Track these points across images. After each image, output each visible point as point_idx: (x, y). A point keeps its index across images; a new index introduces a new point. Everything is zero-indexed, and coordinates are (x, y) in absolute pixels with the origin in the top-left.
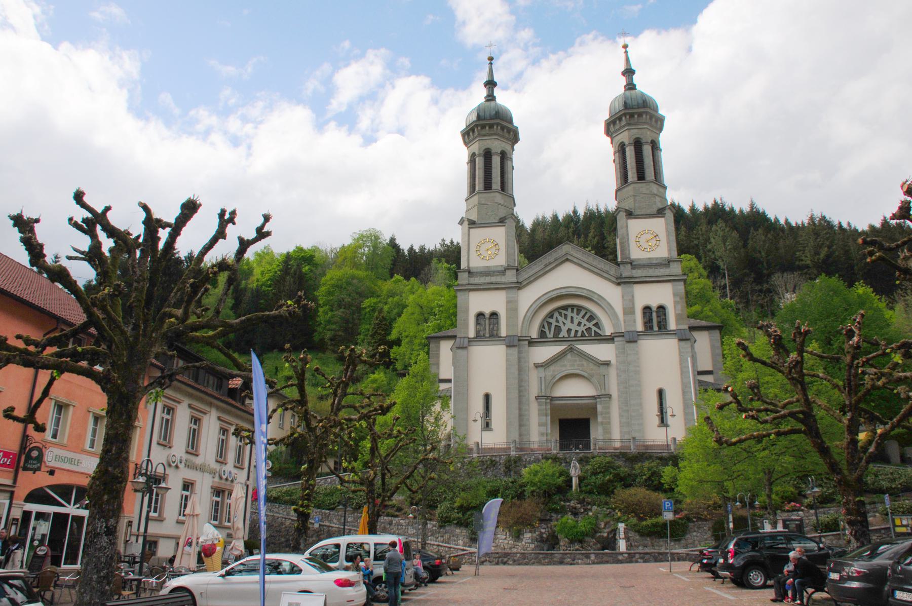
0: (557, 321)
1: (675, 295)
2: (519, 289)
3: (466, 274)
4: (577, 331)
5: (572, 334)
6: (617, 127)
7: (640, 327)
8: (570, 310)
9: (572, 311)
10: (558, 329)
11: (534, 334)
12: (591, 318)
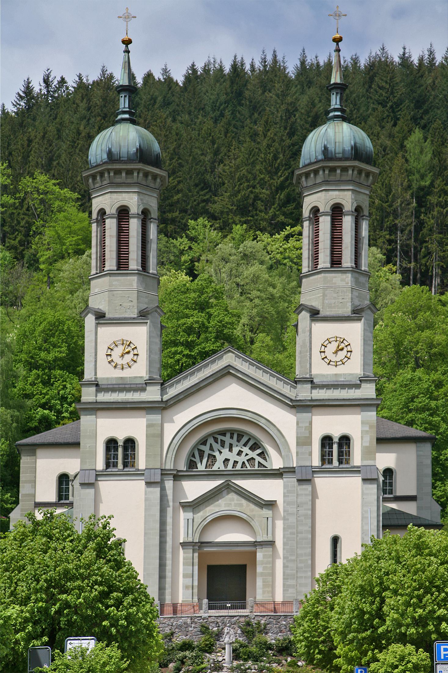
0: (211, 448)
4: (236, 462)
5: (230, 467)
8: (228, 435)
9: (232, 437)
10: (212, 458)
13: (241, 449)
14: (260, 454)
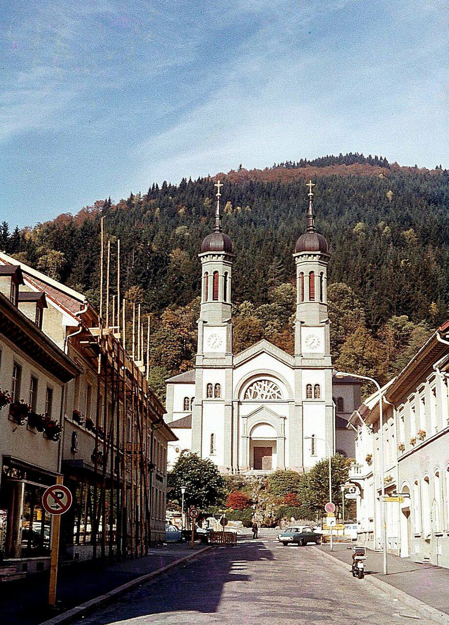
0: (255, 389)
10: (256, 394)
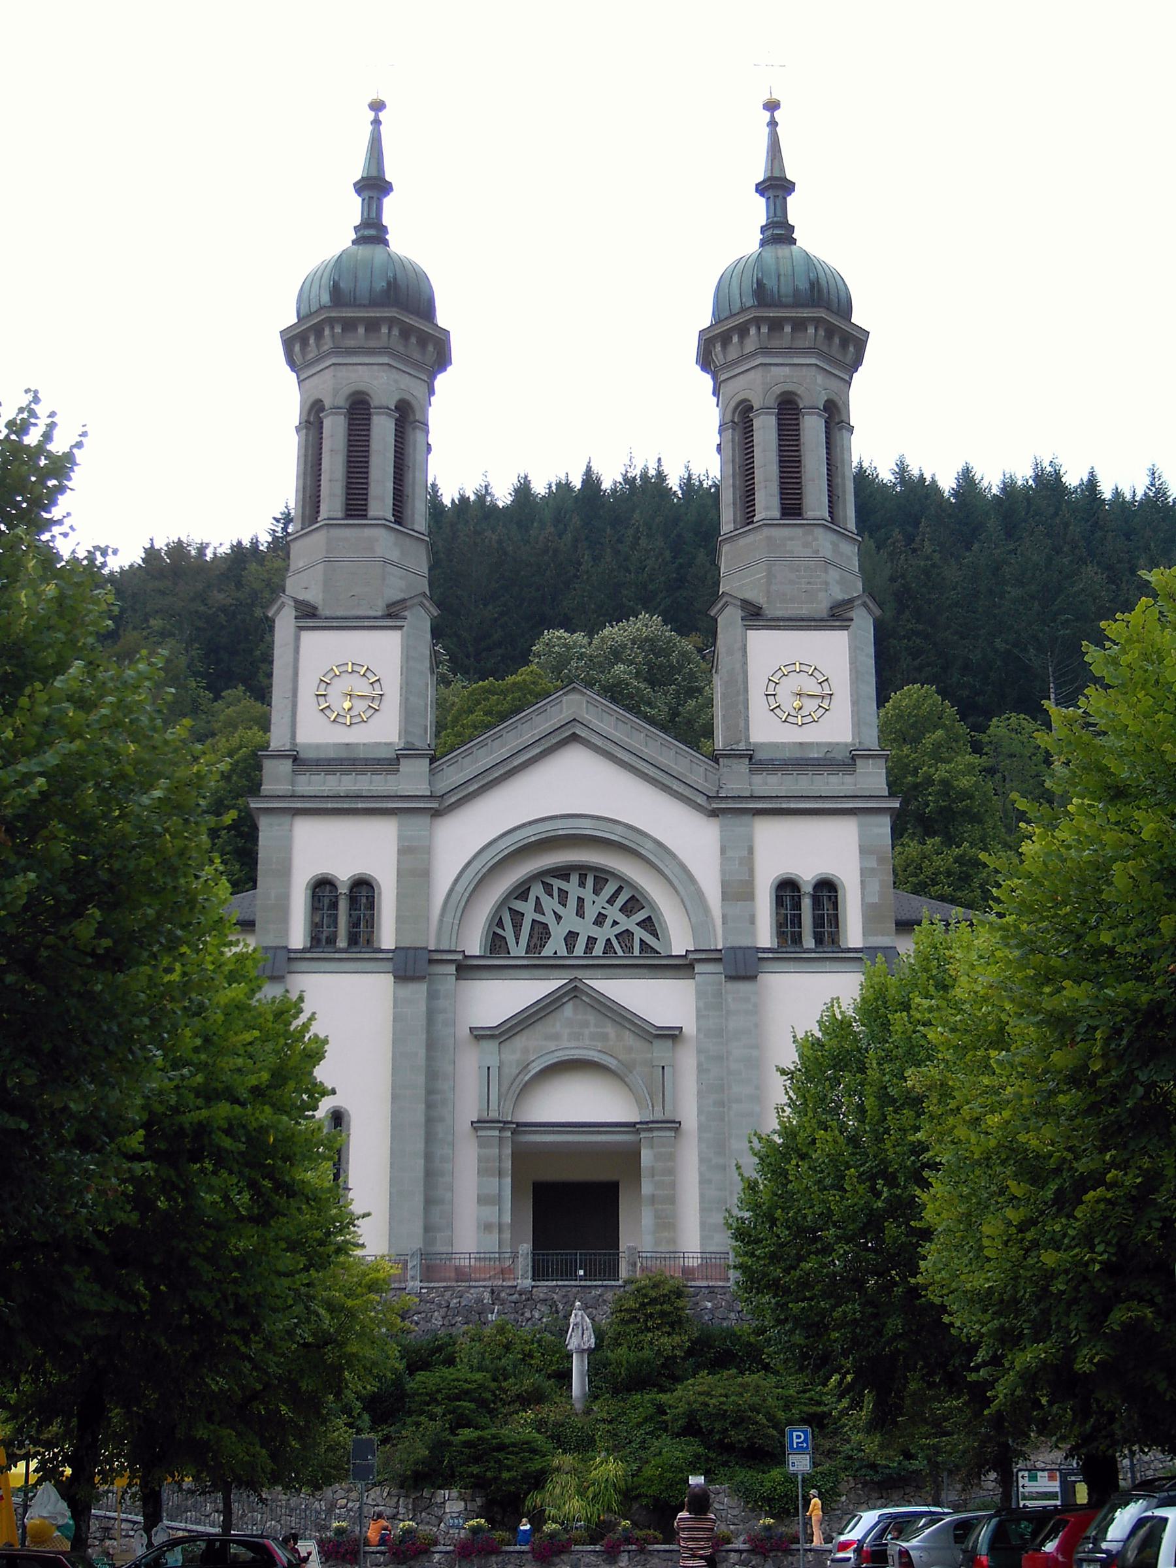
0: (539, 908)
1: (864, 851)
2: (437, 814)
3: (287, 765)
4: (592, 941)
5: (579, 950)
6: (733, 353)
7: (765, 937)
8: (574, 878)
9: (582, 884)
10: (541, 933)
11: (474, 944)
12: (634, 904)
13: (603, 911)
14: (643, 921)
